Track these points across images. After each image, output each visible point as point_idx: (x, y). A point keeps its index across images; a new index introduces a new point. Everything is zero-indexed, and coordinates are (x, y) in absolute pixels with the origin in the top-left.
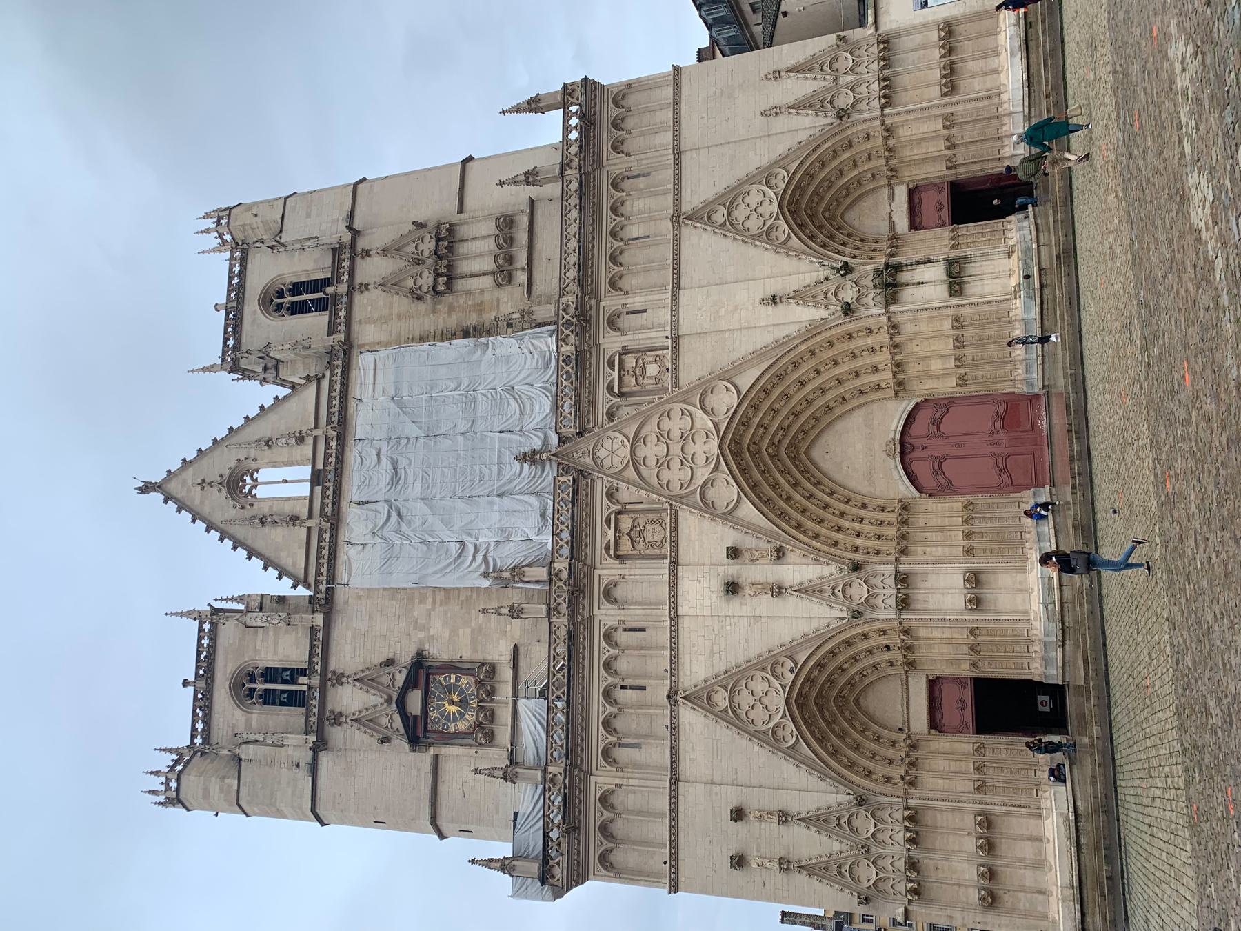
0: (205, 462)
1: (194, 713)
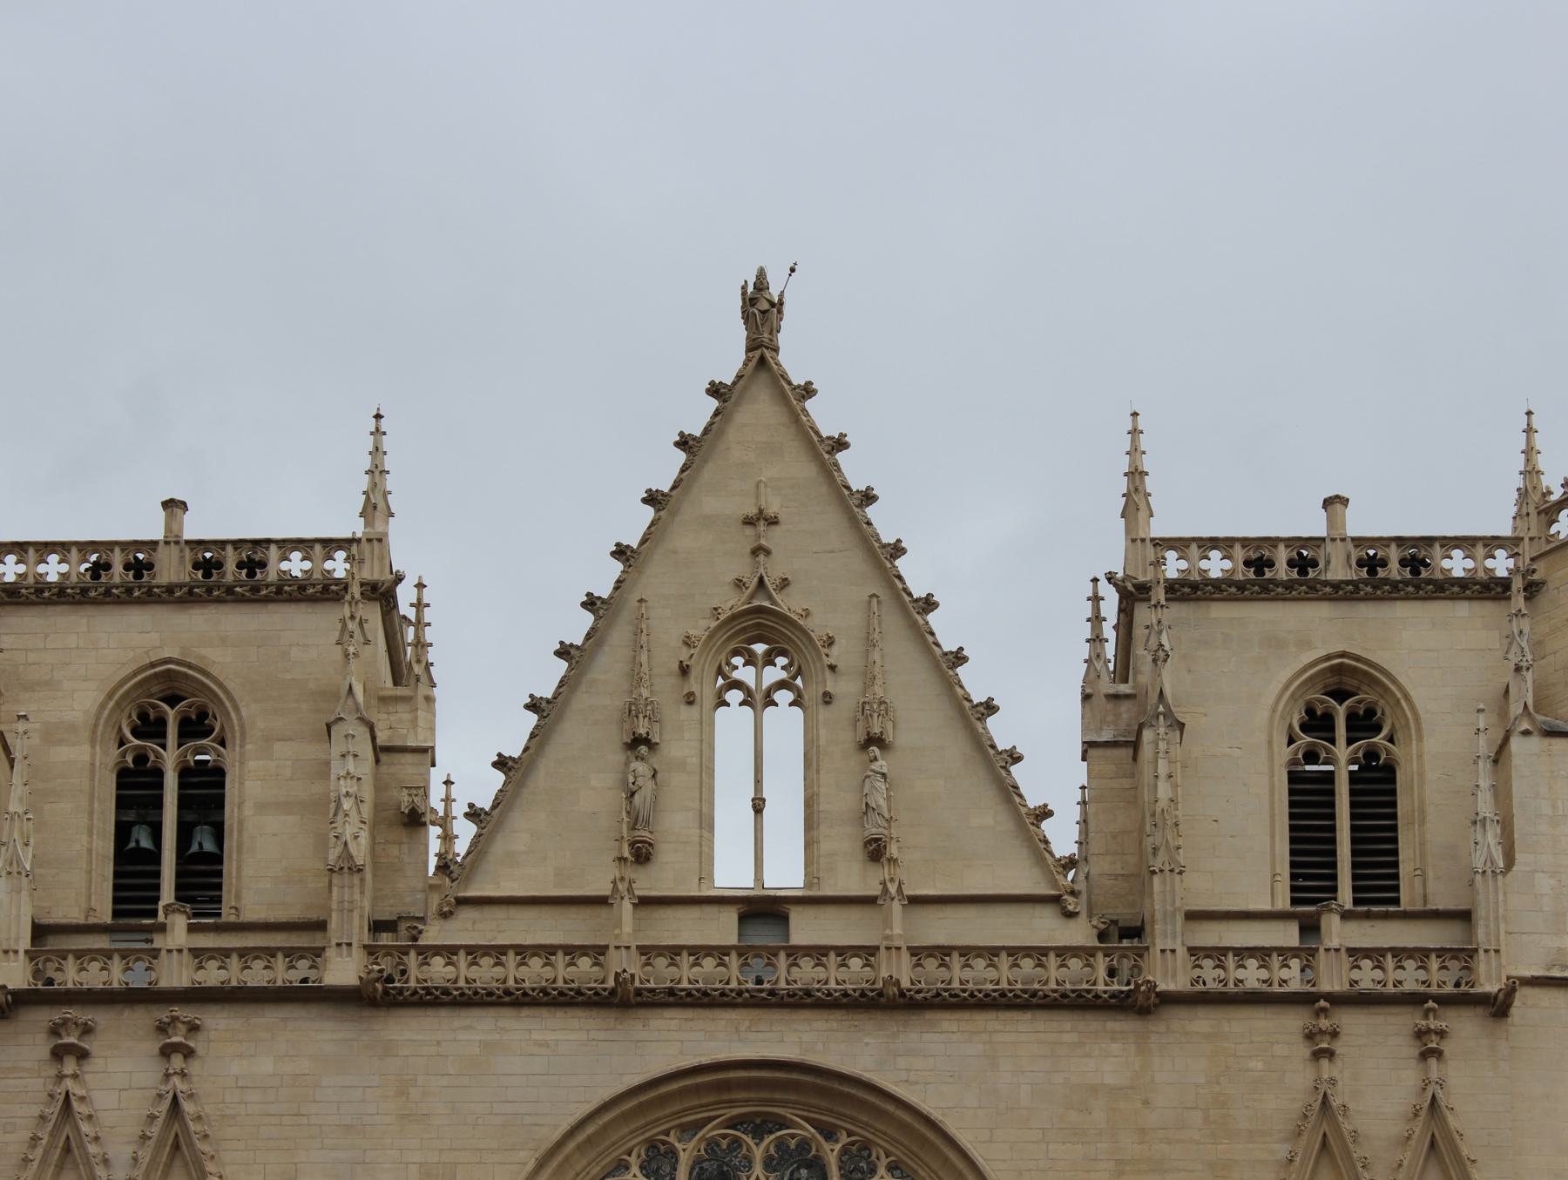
0: (830, 520)
1: (85, 547)
